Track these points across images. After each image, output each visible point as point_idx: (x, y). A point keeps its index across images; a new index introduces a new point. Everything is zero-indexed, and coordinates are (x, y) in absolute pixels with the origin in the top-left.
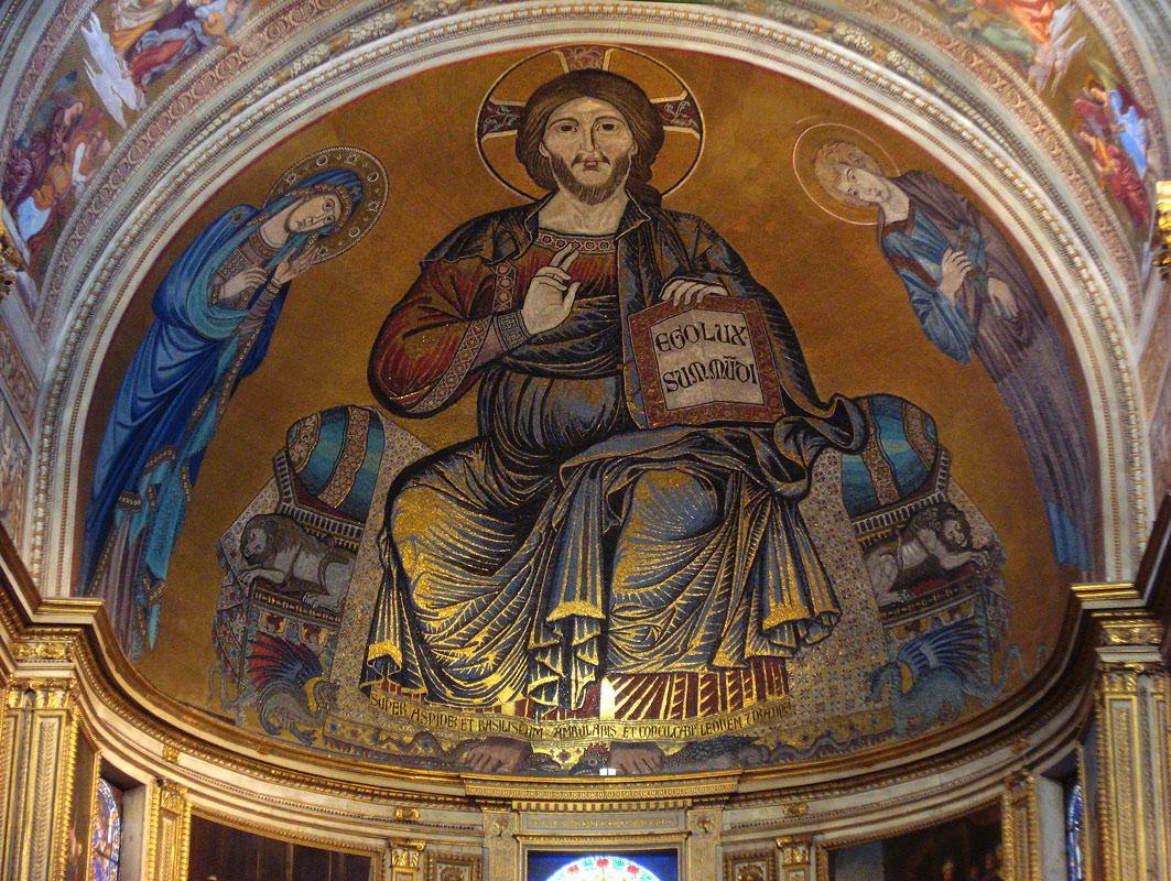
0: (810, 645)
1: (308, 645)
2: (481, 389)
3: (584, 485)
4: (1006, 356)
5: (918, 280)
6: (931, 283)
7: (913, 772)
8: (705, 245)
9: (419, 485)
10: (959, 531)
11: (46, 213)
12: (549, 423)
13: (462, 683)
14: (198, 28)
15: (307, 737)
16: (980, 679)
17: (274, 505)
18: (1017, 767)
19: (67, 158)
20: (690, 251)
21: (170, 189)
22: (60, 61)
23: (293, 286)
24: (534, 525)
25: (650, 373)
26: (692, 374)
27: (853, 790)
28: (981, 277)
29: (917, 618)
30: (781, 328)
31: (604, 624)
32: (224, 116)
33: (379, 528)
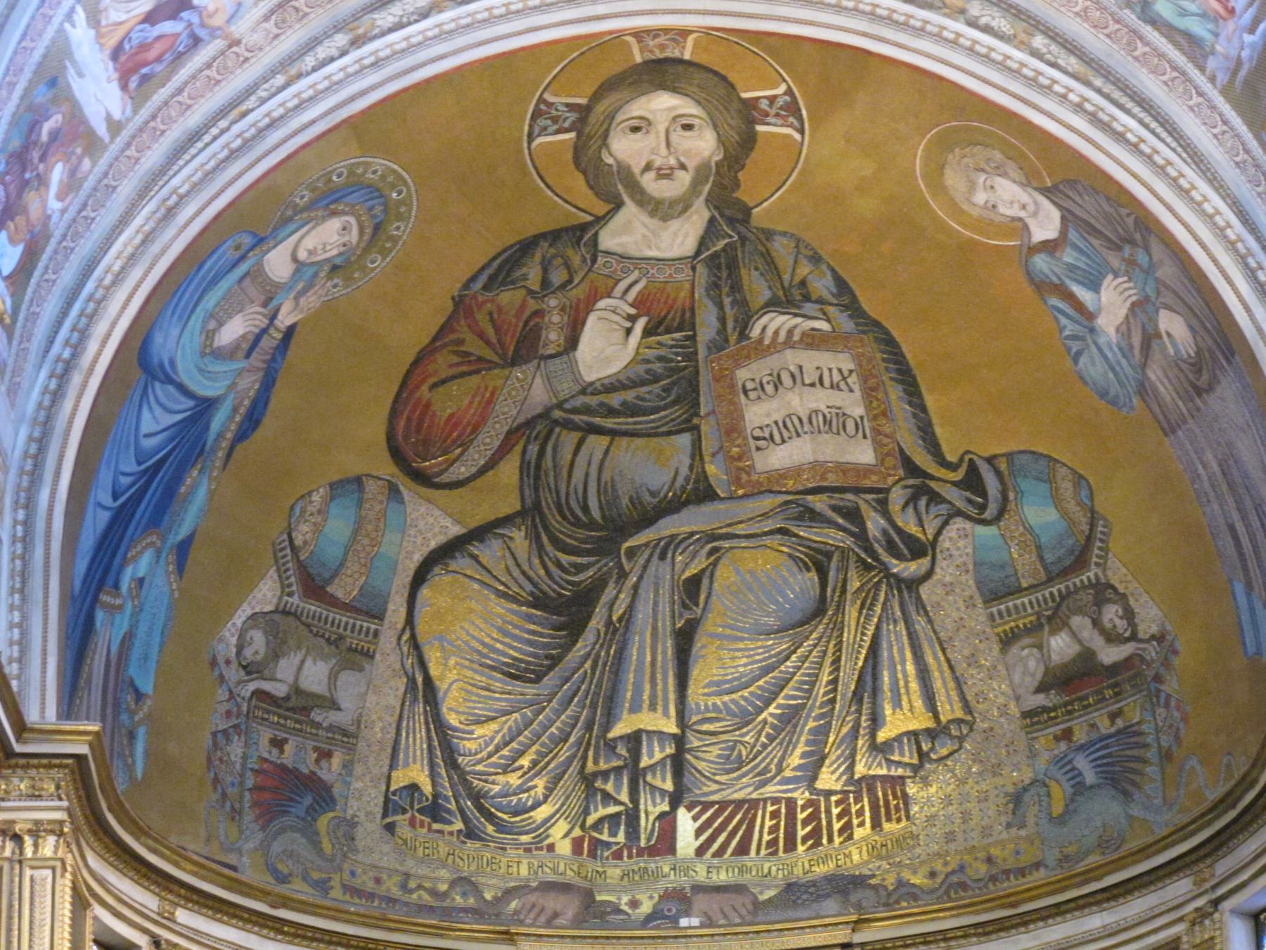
0: (936, 761)
1: (319, 773)
2: (524, 452)
3: (652, 569)
4: (1180, 403)
5: (1070, 311)
6: (1086, 315)
7: (1067, 912)
8: (804, 270)
9: (448, 572)
10: (1121, 618)
11: (20, 249)
12: (608, 491)
13: (505, 817)
14: (195, 19)
15: (323, 886)
16: (1148, 797)
17: (275, 601)
18: (1200, 902)
19: (42, 181)
20: (786, 277)
21: (159, 215)
22: (40, 65)
23: (298, 329)
24: (589, 617)
25: (733, 428)
26: (788, 429)
27: (994, 936)
28: (1150, 308)
29: (1069, 724)
30: (899, 371)
31: (679, 741)
32: (223, 124)
33: (400, 626)
